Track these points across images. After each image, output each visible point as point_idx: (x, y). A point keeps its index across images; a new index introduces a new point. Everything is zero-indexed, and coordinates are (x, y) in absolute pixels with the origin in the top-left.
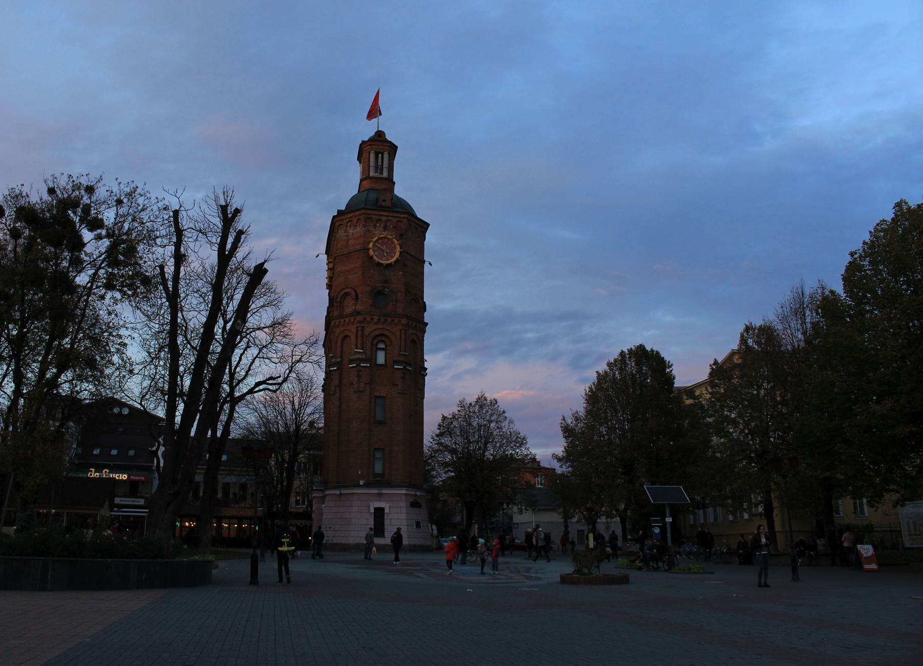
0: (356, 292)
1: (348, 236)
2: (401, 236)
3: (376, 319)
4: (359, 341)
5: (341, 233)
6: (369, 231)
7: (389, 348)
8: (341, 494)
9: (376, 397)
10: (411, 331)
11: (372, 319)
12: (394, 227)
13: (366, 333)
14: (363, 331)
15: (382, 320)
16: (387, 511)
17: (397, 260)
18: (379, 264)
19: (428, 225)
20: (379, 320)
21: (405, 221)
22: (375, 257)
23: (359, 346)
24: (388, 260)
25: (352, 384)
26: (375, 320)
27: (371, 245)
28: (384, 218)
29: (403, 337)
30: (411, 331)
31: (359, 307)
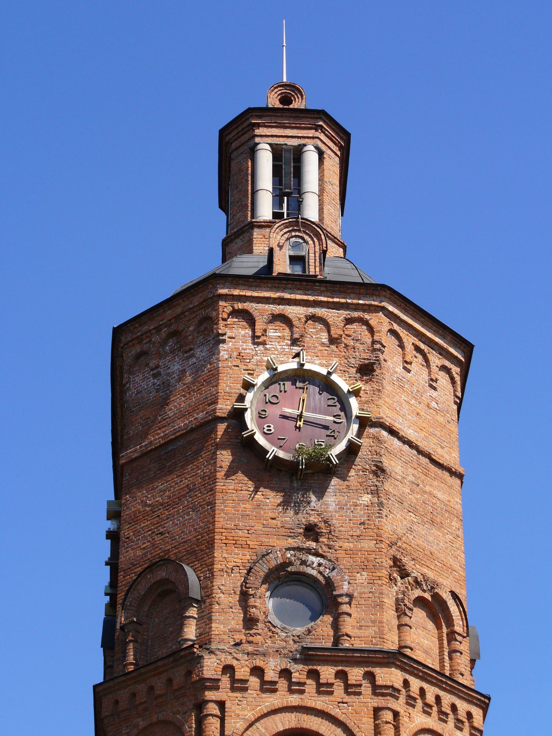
2: (367, 370)
3: (272, 668)
5: (141, 383)
11: (258, 671)
17: (352, 450)
19: (467, 348)
20: (286, 673)
28: (294, 312)
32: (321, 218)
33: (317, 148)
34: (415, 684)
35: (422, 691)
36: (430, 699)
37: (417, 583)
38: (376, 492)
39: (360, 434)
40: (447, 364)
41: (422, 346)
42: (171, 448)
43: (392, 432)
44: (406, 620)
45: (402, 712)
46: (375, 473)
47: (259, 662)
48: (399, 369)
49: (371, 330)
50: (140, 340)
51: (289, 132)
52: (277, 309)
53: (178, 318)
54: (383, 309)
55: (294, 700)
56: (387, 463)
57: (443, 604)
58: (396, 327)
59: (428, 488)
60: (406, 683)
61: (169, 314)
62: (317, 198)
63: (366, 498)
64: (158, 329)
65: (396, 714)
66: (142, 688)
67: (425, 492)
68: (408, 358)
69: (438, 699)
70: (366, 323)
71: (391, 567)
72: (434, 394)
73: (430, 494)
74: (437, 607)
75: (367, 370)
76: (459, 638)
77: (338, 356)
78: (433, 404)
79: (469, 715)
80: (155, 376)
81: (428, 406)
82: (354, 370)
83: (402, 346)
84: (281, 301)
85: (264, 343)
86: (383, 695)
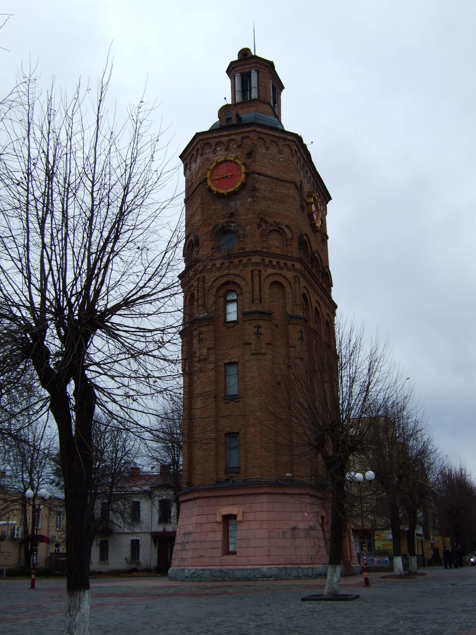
1: (192, 173)
6: (208, 160)
7: (240, 298)
9: (226, 364)
10: (270, 271)
12: (239, 146)
14: (204, 282)
15: (226, 264)
16: (239, 518)
17: (244, 185)
18: (219, 195)
20: (223, 264)
26: (218, 265)
27: (208, 176)
28: (225, 139)
29: (256, 280)
30: (270, 271)
32: (259, 96)
33: (255, 70)
34: (267, 260)
35: (270, 261)
36: (274, 263)
37: (271, 225)
38: (252, 197)
40: (287, 143)
41: (275, 140)
43: (259, 174)
44: (265, 239)
45: (262, 270)
46: (253, 191)
47: (214, 262)
48: (264, 151)
49: (251, 140)
51: (246, 67)
52: (218, 140)
54: (255, 131)
55: (225, 272)
56: (257, 186)
57: (283, 230)
58: (261, 136)
59: (277, 191)
60: (263, 260)
62: (257, 89)
65: (260, 271)
67: (276, 192)
68: (268, 146)
69: (278, 262)
70: (249, 137)
71: (259, 222)
72: (282, 156)
73: (279, 192)
74: (280, 231)
75: (250, 154)
76: (289, 240)
78: (281, 159)
79: (293, 265)
81: (279, 161)
82: (245, 156)
83: (265, 142)
84: (220, 136)
85: (215, 153)
86: (254, 265)
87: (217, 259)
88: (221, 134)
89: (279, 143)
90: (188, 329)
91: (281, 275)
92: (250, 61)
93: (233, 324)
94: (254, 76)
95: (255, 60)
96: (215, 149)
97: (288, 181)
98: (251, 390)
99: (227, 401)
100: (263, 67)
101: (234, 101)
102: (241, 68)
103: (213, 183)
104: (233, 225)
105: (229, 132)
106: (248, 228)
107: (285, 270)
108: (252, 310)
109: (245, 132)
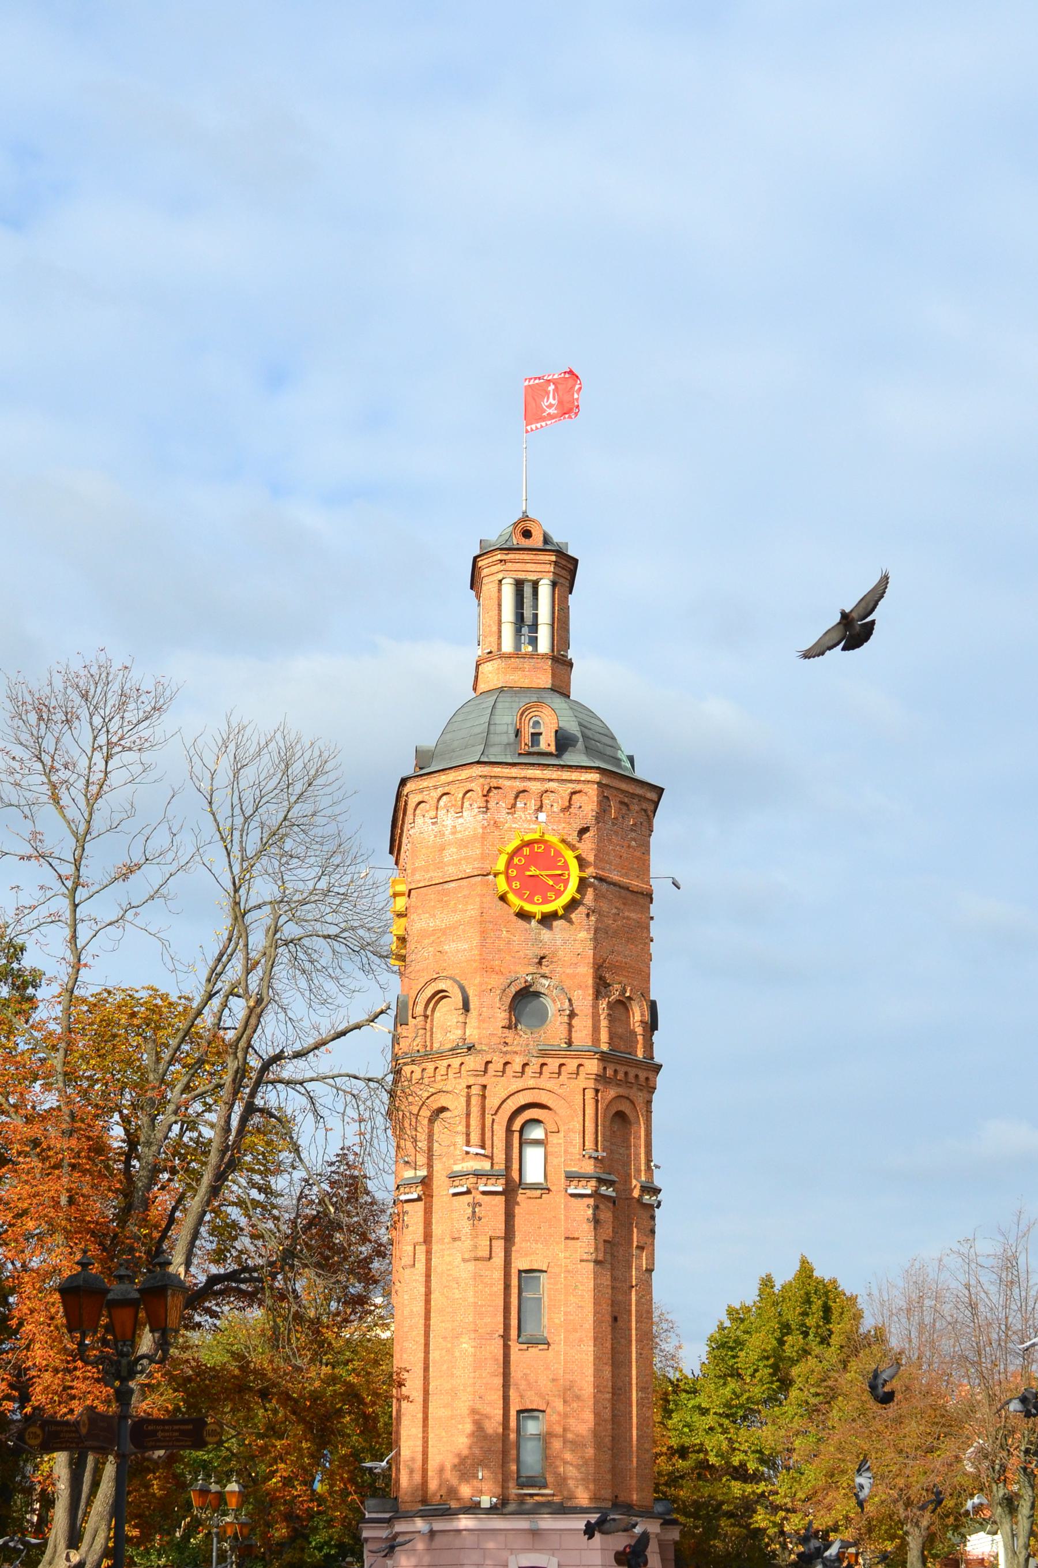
0: (463, 990)
1: (442, 834)
4: (475, 1122)
7: (553, 1139)
8: (432, 1533)
13: (492, 1102)
14: (484, 1097)
18: (523, 915)
19: (660, 791)
20: (525, 1065)
21: (592, 791)
22: (511, 897)
23: (475, 1138)
24: (546, 901)
25: (455, 1239)
28: (535, 787)
31: (472, 1033)
36: (621, 1076)
39: (578, 891)
40: (645, 806)
41: (626, 800)
42: (446, 886)
47: (508, 1058)
50: (421, 791)
53: (449, 783)
55: (531, 1083)
59: (627, 914)
60: (605, 1068)
61: (443, 778)
63: (583, 935)
64: (436, 788)
66: (430, 1066)
69: (626, 1073)
72: (634, 835)
73: (628, 918)
77: (565, 822)
80: (433, 824)
81: (629, 846)
85: (513, 814)
87: (516, 1053)
88: (531, 772)
89: (632, 807)
90: (426, 1180)
91: (628, 1098)
92: (541, 557)
93: (539, 1192)
94: (545, 591)
95: (553, 558)
96: (514, 806)
97: (642, 894)
98: (575, 1330)
99: (525, 1346)
100: (564, 573)
101: (494, 639)
102: (518, 566)
103: (510, 885)
104: (546, 982)
105: (548, 773)
106: (577, 995)
107: (635, 1089)
108: (583, 1171)
109: (579, 781)
